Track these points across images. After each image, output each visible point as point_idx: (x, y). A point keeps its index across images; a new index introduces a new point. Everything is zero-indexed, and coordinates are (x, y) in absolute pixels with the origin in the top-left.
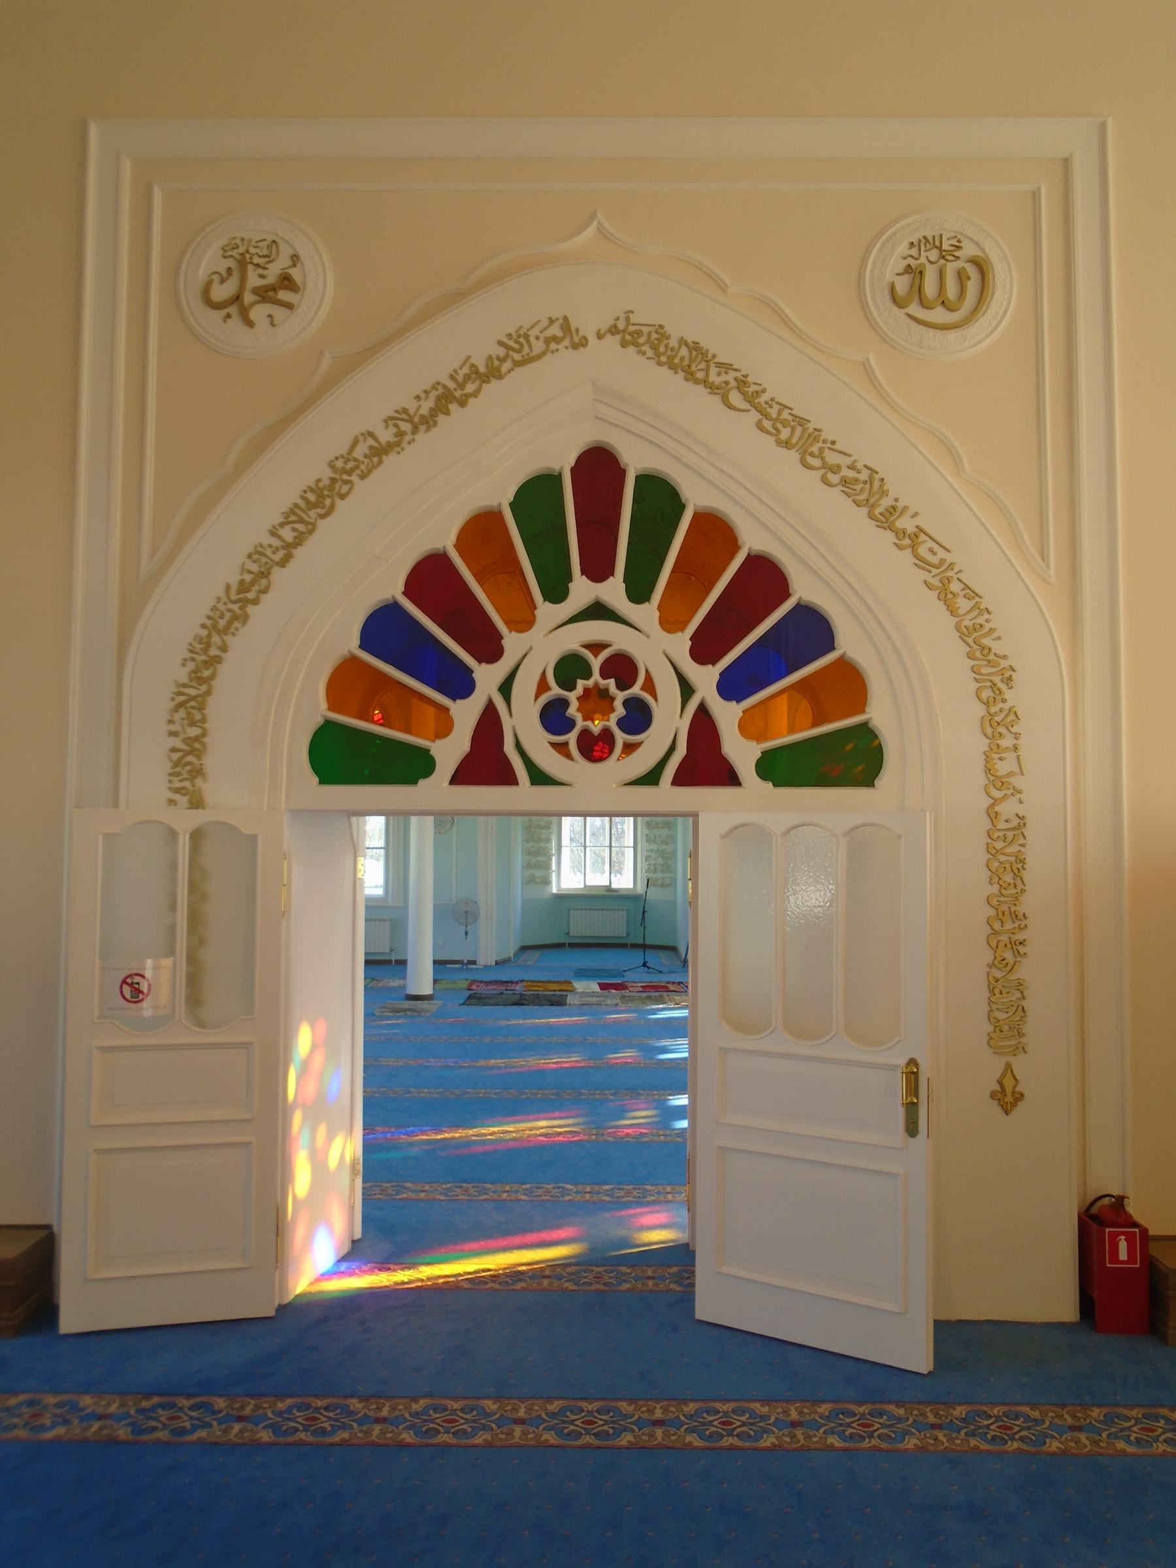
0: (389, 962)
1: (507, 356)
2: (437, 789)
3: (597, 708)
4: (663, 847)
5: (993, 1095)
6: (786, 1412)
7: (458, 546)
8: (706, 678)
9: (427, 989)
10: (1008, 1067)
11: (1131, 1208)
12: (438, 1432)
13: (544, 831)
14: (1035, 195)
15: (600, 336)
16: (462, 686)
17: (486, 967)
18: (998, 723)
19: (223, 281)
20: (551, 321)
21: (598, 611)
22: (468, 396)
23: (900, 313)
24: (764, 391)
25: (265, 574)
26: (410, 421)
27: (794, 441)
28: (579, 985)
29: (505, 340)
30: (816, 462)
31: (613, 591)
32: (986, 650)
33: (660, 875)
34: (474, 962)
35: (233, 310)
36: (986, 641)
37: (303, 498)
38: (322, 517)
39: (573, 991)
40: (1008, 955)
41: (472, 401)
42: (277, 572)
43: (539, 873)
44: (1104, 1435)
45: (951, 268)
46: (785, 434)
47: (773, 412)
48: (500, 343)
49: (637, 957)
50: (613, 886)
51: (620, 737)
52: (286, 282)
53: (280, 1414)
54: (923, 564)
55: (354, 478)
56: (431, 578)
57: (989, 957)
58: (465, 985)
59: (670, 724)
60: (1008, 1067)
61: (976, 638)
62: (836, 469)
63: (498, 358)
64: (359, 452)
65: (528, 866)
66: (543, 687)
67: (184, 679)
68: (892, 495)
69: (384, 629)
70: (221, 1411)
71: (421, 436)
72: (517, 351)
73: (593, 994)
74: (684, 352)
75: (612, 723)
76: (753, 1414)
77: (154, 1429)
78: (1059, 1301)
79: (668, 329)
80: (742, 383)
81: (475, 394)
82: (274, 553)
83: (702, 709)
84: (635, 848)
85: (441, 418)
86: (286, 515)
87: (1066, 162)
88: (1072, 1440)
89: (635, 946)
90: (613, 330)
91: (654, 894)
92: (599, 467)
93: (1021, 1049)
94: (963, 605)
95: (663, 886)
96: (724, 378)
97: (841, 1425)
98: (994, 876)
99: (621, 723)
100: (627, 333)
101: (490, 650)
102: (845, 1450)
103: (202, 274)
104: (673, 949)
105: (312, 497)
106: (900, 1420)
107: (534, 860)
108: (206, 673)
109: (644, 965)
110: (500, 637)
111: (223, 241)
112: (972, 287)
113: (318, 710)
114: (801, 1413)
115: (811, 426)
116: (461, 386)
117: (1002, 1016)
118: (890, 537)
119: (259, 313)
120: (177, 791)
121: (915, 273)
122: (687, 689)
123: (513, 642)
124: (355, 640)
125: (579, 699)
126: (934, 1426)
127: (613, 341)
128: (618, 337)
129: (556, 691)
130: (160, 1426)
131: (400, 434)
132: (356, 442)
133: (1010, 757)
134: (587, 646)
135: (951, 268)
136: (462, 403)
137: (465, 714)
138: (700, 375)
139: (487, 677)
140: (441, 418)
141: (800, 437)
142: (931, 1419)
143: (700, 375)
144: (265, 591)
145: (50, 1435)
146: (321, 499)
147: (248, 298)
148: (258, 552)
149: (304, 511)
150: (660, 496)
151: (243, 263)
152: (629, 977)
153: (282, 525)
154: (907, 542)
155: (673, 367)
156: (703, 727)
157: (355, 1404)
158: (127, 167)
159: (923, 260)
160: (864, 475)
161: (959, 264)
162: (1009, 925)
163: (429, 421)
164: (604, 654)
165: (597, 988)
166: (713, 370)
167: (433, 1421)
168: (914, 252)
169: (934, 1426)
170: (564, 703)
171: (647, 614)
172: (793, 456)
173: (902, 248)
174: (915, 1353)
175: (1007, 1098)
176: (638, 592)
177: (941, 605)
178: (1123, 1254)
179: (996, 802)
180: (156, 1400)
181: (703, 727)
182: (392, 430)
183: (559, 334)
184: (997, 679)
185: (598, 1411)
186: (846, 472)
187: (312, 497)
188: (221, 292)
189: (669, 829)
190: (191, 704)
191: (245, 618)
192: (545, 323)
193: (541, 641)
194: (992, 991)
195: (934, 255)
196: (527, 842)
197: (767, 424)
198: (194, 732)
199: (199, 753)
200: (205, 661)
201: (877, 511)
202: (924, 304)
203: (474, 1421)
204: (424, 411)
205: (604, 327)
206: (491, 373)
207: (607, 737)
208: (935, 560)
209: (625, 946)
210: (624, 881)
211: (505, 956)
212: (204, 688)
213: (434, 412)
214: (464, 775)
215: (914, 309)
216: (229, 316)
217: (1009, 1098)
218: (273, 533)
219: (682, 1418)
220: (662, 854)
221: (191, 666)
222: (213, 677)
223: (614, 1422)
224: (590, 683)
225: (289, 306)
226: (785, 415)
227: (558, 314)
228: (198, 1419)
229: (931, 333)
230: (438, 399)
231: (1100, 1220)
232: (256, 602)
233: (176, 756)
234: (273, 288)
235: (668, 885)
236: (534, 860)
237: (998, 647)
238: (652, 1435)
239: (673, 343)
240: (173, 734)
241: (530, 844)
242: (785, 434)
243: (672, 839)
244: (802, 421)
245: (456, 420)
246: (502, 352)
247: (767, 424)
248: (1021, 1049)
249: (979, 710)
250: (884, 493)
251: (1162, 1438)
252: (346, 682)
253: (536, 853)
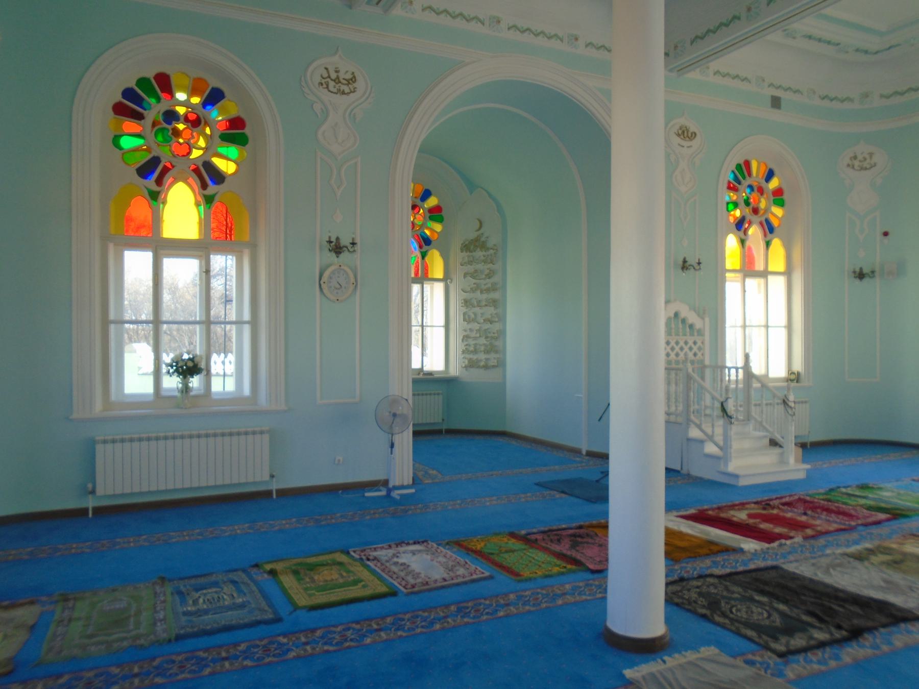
0: (268, 494)
4: (487, 326)
33: (482, 356)
84: (447, 327)
95: (486, 367)
189: (496, 307)
209: (438, 432)
220: (485, 334)
243: (502, 318)
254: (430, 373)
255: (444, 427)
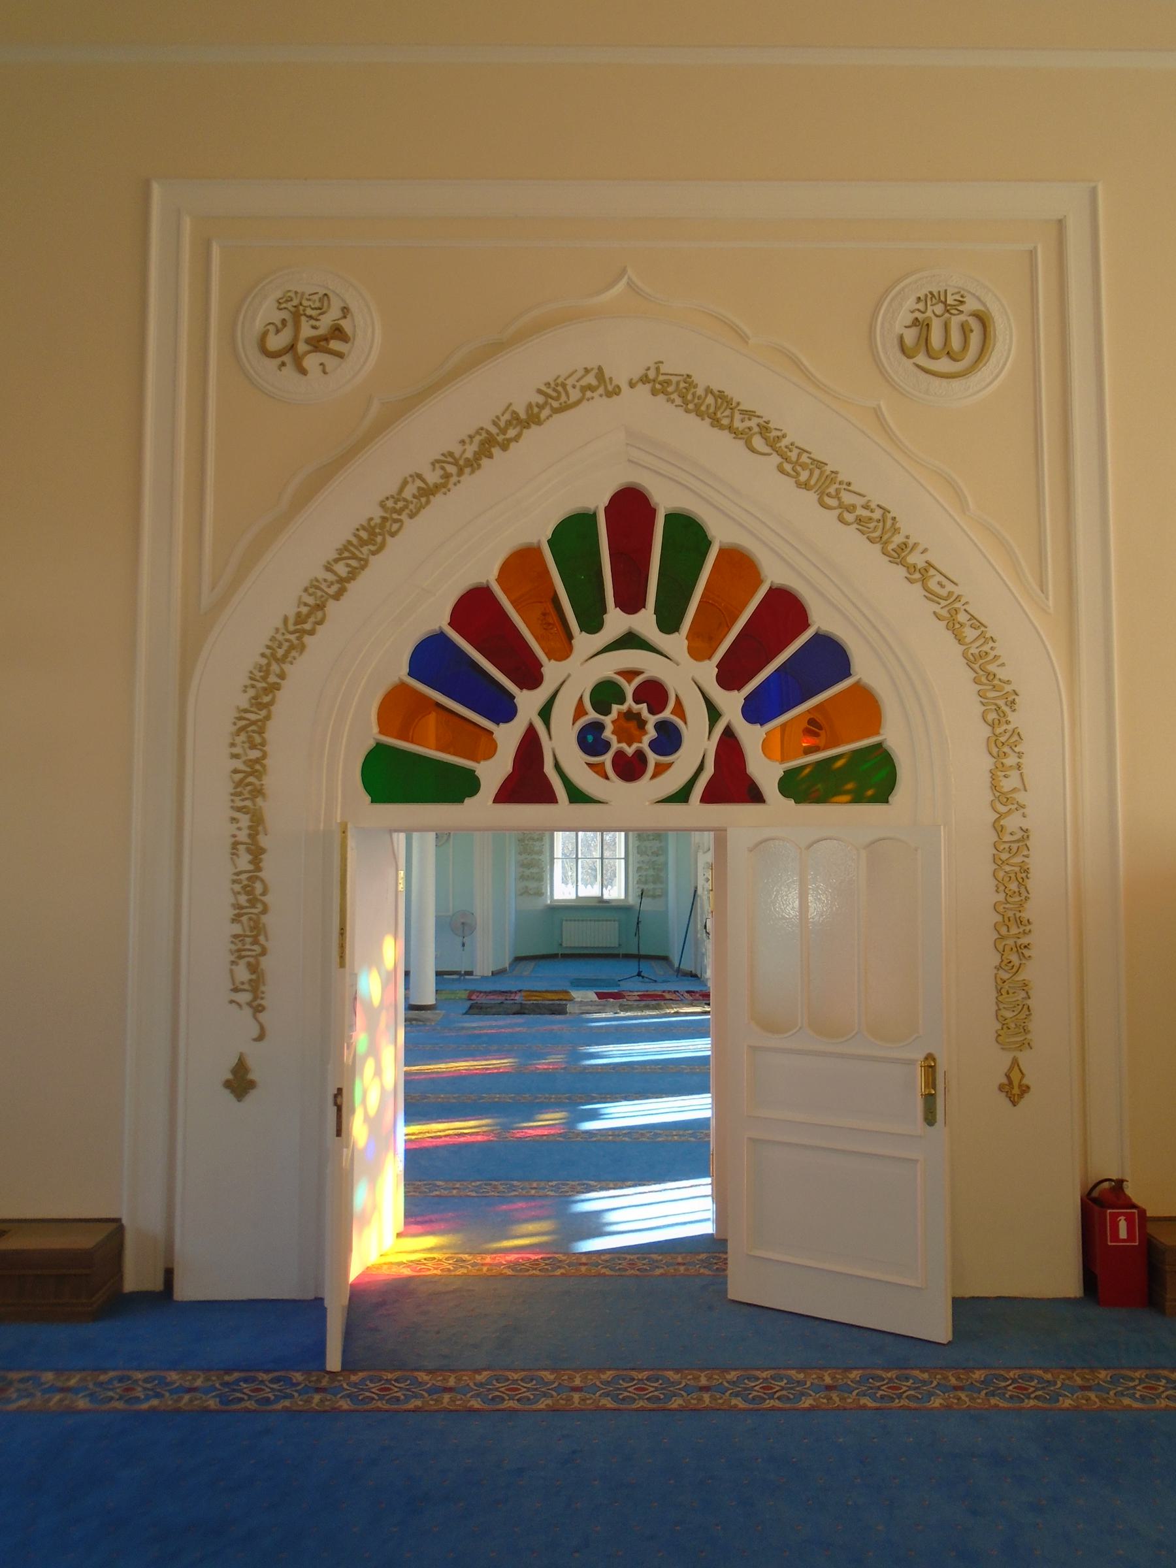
1: (546, 403)
2: (480, 808)
3: (630, 732)
4: (654, 858)
5: (1001, 1088)
6: (821, 1378)
7: (499, 580)
8: (732, 703)
9: (430, 999)
10: (1015, 1062)
11: (1130, 1190)
12: (503, 1399)
13: (537, 843)
14: (1032, 254)
15: (632, 385)
16: (504, 710)
17: (483, 977)
18: (1003, 743)
19: (278, 331)
20: (587, 371)
21: (630, 641)
22: (509, 440)
23: (908, 363)
24: (784, 436)
25: (320, 607)
26: (456, 463)
27: (813, 482)
28: (578, 995)
29: (544, 389)
30: (832, 502)
31: (645, 622)
32: (991, 676)
34: (470, 973)
35: (287, 358)
36: (991, 668)
37: (355, 535)
38: (374, 553)
39: (571, 1000)
40: (1014, 958)
41: (513, 445)
42: (331, 605)
43: (532, 885)
44: (1112, 1393)
45: (955, 321)
46: (804, 476)
47: (793, 455)
48: (539, 391)
49: (631, 967)
50: (606, 897)
51: (652, 758)
52: (338, 332)
53: (355, 1385)
54: (931, 596)
55: (404, 517)
56: (475, 610)
57: (996, 959)
58: (464, 995)
59: (699, 744)
60: (1015, 1062)
61: (982, 664)
62: (851, 509)
63: (538, 405)
64: (408, 493)
65: (522, 878)
66: (580, 711)
67: (245, 705)
68: (903, 532)
69: (432, 658)
70: (299, 1384)
71: (465, 478)
72: (555, 399)
73: (592, 1003)
74: (710, 400)
75: (645, 745)
76: (790, 1380)
77: (241, 1400)
78: (1064, 1279)
79: (696, 379)
80: (764, 429)
81: (516, 439)
82: (329, 587)
83: (729, 733)
84: (626, 859)
85: (485, 462)
86: (340, 551)
87: (1061, 223)
88: (1083, 1398)
89: (628, 956)
90: (644, 379)
91: (648, 905)
92: (630, 507)
93: (1026, 1045)
94: (970, 634)
95: (654, 897)
96: (747, 424)
97: (871, 1388)
98: (1001, 886)
99: (653, 745)
100: (658, 383)
101: (530, 677)
102: (877, 1409)
103: (258, 325)
104: (665, 959)
105: (364, 535)
106: (924, 1382)
107: (527, 872)
108: (266, 699)
109: (639, 974)
110: (539, 665)
111: (279, 294)
112: (975, 339)
113: (371, 734)
114: (833, 1378)
115: (828, 469)
116: (504, 431)
117: (1008, 1014)
118: (901, 571)
119: (312, 361)
120: (239, 809)
121: (922, 326)
122: (714, 713)
123: (552, 670)
124: (405, 669)
125: (613, 722)
126: (956, 1388)
127: (643, 390)
128: (648, 386)
129: (593, 715)
130: (246, 1397)
131: (447, 476)
132: (405, 483)
133: (1014, 774)
134: (620, 673)
135: (955, 321)
136: (504, 447)
137: (508, 736)
138: (725, 422)
139: (528, 702)
140: (485, 462)
141: (817, 479)
142: (953, 1381)
143: (725, 422)
144: (320, 623)
145: (145, 1406)
146: (372, 537)
147: (302, 347)
148: (314, 586)
149: (356, 548)
150: (688, 534)
151: (296, 315)
152: (625, 986)
153: (336, 561)
154: (917, 576)
155: (700, 414)
156: (729, 749)
157: (423, 1376)
158: (187, 223)
159: (929, 313)
160: (877, 515)
161: (962, 318)
162: (1014, 930)
163: (473, 464)
164: (637, 681)
165: (595, 998)
166: (737, 416)
167: (497, 1389)
168: (921, 306)
169: (956, 1388)
170: (598, 727)
171: (677, 643)
172: (812, 497)
173: (910, 303)
174: (937, 1326)
175: (1014, 1090)
176: (668, 622)
177: (949, 636)
178: (1123, 1234)
179: (1001, 816)
180: (236, 1375)
181: (729, 749)
182: (439, 472)
183: (594, 382)
184: (1001, 703)
185: (648, 1379)
186: (860, 512)
187: (364, 535)
188: (276, 342)
189: (661, 841)
190: (252, 726)
191: (302, 648)
192: (581, 372)
193: (577, 671)
194: (999, 991)
195: (939, 309)
196: (520, 854)
197: (788, 467)
198: (254, 754)
199: (259, 775)
200: (265, 688)
201: (890, 547)
202: (931, 355)
203: (536, 1389)
204: (469, 454)
205: (637, 374)
206: (531, 419)
207: (640, 756)
208: (943, 592)
210: (616, 892)
211: (500, 967)
212: (264, 713)
213: (478, 456)
214: (509, 793)
215: (921, 359)
216: (283, 364)
217: (1016, 1091)
218: (328, 568)
219: (726, 1384)
221: (251, 692)
222: (272, 703)
223: (663, 1389)
224: (624, 708)
225: (340, 355)
226: (804, 458)
227: (592, 364)
228: (279, 1391)
229: (936, 382)
230: (482, 443)
231: (1101, 1203)
232: (312, 633)
233: (238, 776)
234: (326, 339)
235: (660, 896)
236: (527, 872)
237: (1002, 674)
238: (700, 1399)
239: (700, 391)
240: (235, 756)
241: (524, 856)
242: (804, 476)
243: (662, 851)
244: (820, 465)
245: (498, 464)
246: (541, 399)
247: (788, 467)
248: (1026, 1045)
249: (986, 731)
250: (896, 531)
251: (1164, 1395)
252: (399, 709)
253: (529, 865)
254: (607, 902)
255: (622, 951)
